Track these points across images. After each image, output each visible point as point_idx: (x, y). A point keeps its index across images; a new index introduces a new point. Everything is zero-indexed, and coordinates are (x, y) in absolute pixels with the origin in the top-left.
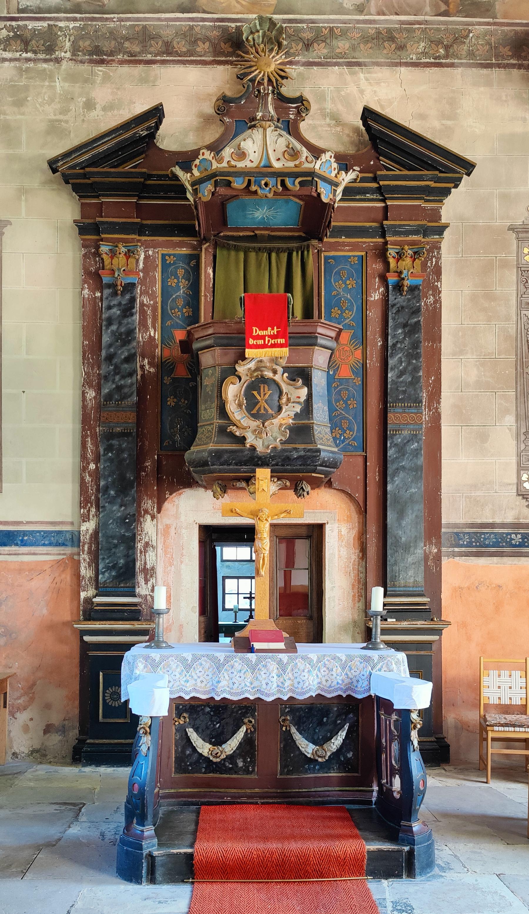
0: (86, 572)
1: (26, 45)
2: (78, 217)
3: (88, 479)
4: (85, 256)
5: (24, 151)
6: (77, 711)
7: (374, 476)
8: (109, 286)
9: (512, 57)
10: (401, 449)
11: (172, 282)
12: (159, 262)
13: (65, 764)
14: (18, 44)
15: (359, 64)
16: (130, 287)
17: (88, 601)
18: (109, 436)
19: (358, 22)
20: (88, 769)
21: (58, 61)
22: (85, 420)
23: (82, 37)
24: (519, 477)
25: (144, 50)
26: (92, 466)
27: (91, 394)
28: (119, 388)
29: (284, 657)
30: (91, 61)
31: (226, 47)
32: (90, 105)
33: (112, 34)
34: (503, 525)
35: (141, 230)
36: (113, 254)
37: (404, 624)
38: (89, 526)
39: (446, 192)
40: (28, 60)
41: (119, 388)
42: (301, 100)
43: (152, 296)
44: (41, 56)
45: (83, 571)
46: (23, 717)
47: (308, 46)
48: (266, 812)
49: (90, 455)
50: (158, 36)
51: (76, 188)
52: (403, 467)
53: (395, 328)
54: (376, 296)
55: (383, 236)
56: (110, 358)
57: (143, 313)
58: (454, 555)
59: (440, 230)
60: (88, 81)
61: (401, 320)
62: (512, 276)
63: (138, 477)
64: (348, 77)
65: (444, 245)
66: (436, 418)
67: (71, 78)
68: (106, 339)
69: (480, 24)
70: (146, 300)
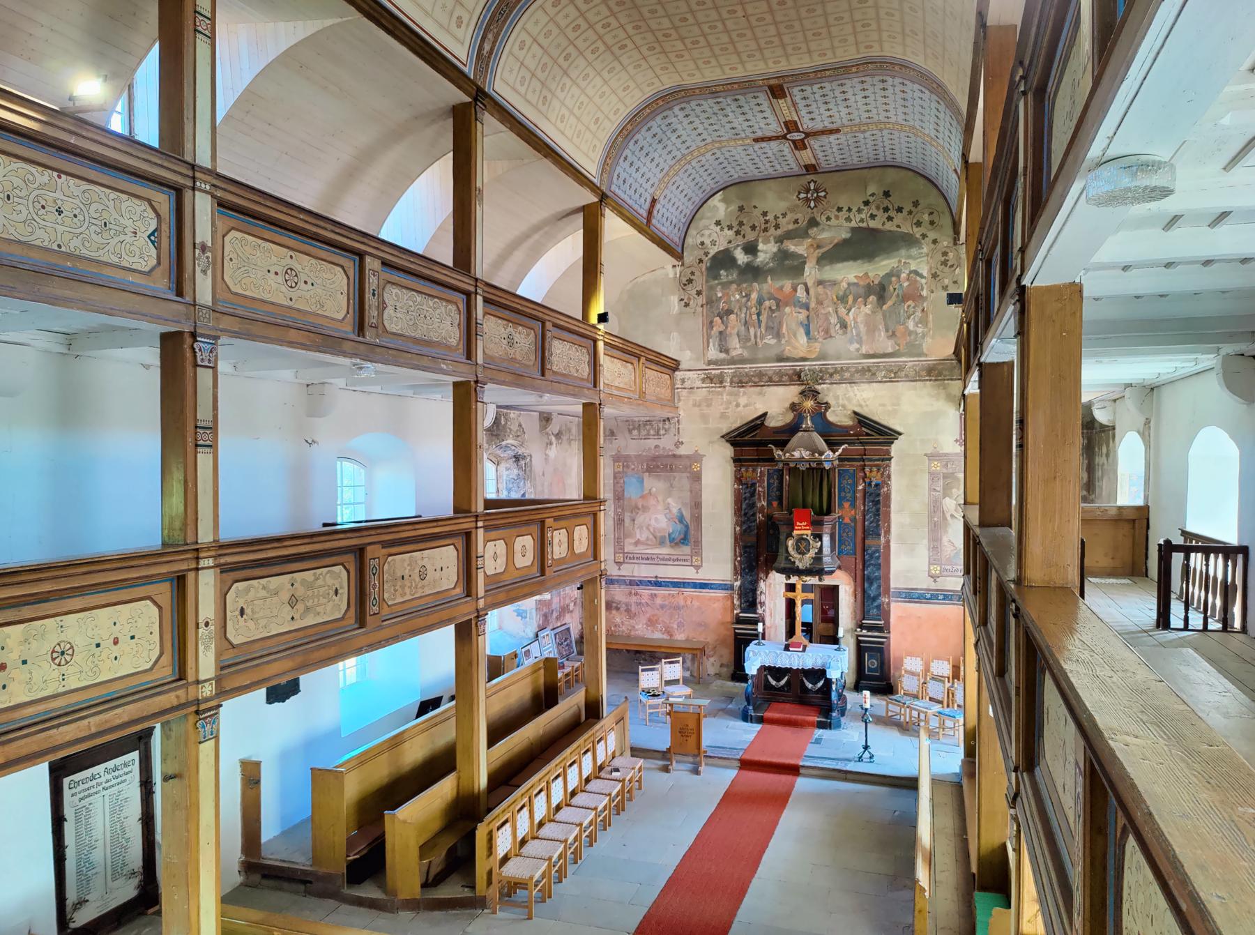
0: (736, 602)
1: (712, 381)
2: (733, 456)
3: (737, 564)
4: (735, 471)
5: (710, 426)
7: (860, 566)
8: (745, 484)
9: (927, 376)
10: (871, 556)
11: (772, 481)
12: (766, 473)
14: (708, 381)
15: (854, 383)
16: (753, 485)
17: (737, 614)
18: (745, 547)
20: (737, 684)
21: (724, 387)
22: (736, 539)
24: (929, 567)
25: (761, 381)
26: (739, 559)
27: (738, 528)
28: (749, 527)
30: (738, 387)
31: (796, 378)
32: (738, 405)
33: (747, 375)
34: (921, 589)
35: (758, 460)
36: (747, 471)
37: (870, 634)
38: (737, 584)
39: (892, 443)
41: (749, 527)
42: (827, 403)
44: (718, 385)
45: (735, 602)
46: (712, 660)
47: (831, 375)
49: (738, 554)
50: (766, 374)
51: (732, 444)
52: (872, 564)
53: (869, 503)
55: (864, 461)
56: (745, 514)
57: (759, 494)
59: (890, 459)
60: (737, 395)
61: (872, 499)
62: (926, 476)
63: (757, 563)
64: (850, 389)
66: (888, 542)
67: (730, 394)
68: (744, 506)
69: (911, 361)
70: (760, 489)
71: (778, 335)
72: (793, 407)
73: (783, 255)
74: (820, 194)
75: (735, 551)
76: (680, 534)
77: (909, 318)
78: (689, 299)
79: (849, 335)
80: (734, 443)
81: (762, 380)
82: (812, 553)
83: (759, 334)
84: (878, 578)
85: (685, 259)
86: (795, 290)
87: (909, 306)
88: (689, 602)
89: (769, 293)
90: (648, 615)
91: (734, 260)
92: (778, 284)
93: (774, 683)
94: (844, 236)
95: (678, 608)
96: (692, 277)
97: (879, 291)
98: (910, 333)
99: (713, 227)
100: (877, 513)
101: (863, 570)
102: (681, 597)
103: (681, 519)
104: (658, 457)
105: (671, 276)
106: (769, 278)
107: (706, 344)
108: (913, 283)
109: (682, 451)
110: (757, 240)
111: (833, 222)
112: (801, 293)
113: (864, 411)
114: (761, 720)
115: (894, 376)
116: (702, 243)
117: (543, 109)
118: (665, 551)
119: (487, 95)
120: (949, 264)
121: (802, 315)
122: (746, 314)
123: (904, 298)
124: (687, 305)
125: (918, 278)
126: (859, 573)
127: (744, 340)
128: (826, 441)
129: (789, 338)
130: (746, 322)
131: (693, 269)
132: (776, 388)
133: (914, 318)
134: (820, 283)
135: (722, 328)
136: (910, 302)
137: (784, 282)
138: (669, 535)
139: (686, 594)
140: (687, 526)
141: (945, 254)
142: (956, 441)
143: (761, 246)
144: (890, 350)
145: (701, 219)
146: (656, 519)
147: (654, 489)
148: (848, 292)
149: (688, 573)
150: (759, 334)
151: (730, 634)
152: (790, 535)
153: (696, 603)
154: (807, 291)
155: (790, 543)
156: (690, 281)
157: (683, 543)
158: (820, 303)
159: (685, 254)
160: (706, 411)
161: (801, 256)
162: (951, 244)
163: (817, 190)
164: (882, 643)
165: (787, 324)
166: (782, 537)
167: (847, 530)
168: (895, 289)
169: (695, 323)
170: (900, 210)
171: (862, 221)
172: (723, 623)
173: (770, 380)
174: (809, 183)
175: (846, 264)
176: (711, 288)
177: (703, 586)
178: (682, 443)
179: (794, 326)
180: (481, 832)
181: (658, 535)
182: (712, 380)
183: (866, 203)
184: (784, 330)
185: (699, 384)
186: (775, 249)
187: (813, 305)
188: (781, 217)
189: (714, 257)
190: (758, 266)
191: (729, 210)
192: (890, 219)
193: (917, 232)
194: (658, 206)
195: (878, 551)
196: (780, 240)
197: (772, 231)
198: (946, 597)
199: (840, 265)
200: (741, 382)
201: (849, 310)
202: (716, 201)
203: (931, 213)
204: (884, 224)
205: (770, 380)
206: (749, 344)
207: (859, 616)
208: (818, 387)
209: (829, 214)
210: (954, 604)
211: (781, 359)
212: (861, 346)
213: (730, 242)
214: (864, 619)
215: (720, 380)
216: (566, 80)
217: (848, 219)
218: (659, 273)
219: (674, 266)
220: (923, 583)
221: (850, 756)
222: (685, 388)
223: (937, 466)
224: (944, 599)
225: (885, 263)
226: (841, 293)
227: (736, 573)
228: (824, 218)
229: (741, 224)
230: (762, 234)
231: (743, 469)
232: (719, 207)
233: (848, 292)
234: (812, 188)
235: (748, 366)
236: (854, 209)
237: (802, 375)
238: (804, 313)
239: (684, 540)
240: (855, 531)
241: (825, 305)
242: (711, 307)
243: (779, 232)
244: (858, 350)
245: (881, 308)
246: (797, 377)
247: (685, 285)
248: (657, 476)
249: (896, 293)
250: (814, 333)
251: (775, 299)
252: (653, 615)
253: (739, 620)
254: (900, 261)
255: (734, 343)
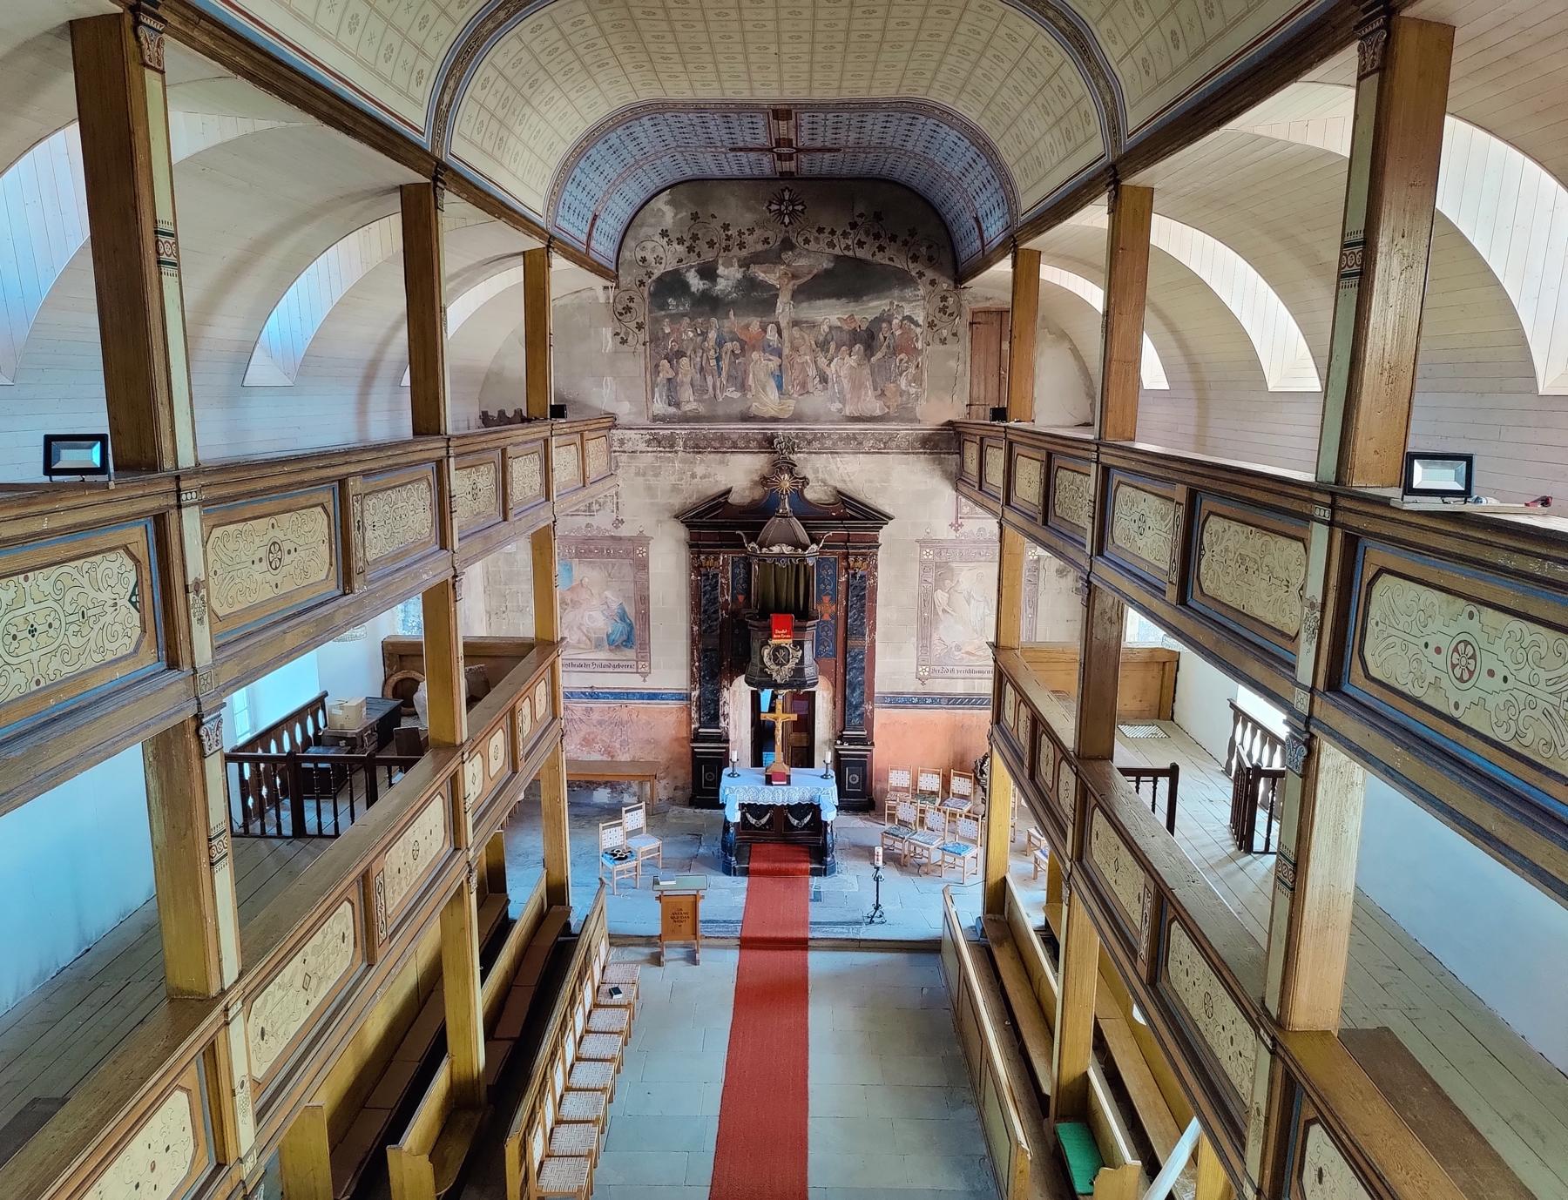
0: (695, 715)
6: (690, 780)
10: (854, 658)
11: (737, 571)
13: (684, 805)
15: (837, 453)
16: (715, 576)
18: (705, 650)
19: (837, 429)
21: (676, 452)
22: (693, 641)
23: (689, 439)
26: (697, 664)
27: (696, 628)
28: (710, 626)
29: (784, 788)
32: (693, 476)
34: (908, 693)
36: (707, 559)
37: (852, 747)
38: (695, 693)
40: (661, 452)
41: (710, 626)
42: (804, 478)
43: (727, 579)
46: (663, 782)
47: (809, 443)
48: (777, 847)
50: (729, 438)
51: (687, 526)
53: (853, 597)
54: (843, 579)
55: (847, 549)
56: (705, 611)
58: (883, 707)
59: (877, 547)
62: (917, 566)
65: (880, 552)
66: (873, 642)
67: (683, 461)
68: (703, 602)
71: (743, 387)
72: (764, 481)
73: (749, 284)
74: (796, 208)
75: (692, 653)
76: (622, 634)
77: (901, 375)
78: (627, 334)
79: (830, 392)
80: (689, 525)
81: (725, 446)
82: (792, 664)
83: (718, 384)
84: (861, 684)
85: (621, 279)
86: (765, 331)
87: (901, 360)
88: (634, 716)
89: (731, 332)
90: (582, 734)
91: (685, 286)
92: (745, 321)
93: (753, 821)
94: (825, 266)
95: (620, 724)
96: (631, 305)
97: (867, 339)
98: (902, 393)
99: (657, 238)
100: (862, 610)
101: (845, 675)
102: (625, 710)
103: (623, 617)
104: (590, 538)
105: (602, 300)
106: (732, 312)
107: (650, 396)
108: (906, 332)
109: (624, 531)
110: (715, 261)
111: (813, 246)
112: (771, 334)
113: (848, 488)
114: (746, 872)
115: (883, 446)
116: (644, 260)
117: (497, 154)
118: (602, 655)
119: (446, 167)
120: (949, 311)
121: (774, 363)
122: (702, 357)
123: (894, 351)
124: (624, 341)
125: (913, 326)
126: (839, 677)
127: (700, 390)
128: (803, 525)
129: (758, 392)
130: (702, 368)
131: (632, 294)
132: (741, 456)
133: (907, 375)
134: (796, 323)
135: (671, 374)
136: (902, 356)
137: (750, 319)
138: (608, 636)
139: (630, 707)
140: (630, 625)
141: (944, 299)
142: (951, 525)
143: (721, 270)
144: (878, 413)
145: (641, 226)
146: (590, 617)
147: (587, 580)
148: (829, 337)
149: (632, 682)
150: (718, 384)
151: (686, 750)
152: (765, 644)
153: (643, 717)
154: (780, 333)
155: (766, 652)
156: (628, 309)
157: (626, 646)
158: (795, 349)
159: (620, 272)
160: (653, 481)
161: (773, 286)
162: (951, 288)
163: (792, 202)
164: (865, 756)
165: (754, 374)
166: (755, 645)
167: (826, 629)
168: (885, 338)
169: (635, 365)
170: (893, 239)
171: (847, 248)
172: (677, 739)
173: (735, 445)
174: (783, 191)
175: (827, 301)
176: (656, 321)
177: (653, 696)
178: (622, 522)
179: (762, 375)
180: (512, 1148)
181: (593, 635)
182: (659, 443)
183: (853, 226)
184: (751, 381)
185: (642, 446)
186: (739, 276)
187: (786, 351)
188: (747, 233)
189: (660, 279)
190: (717, 295)
191: (679, 216)
192: (881, 249)
193: (914, 269)
194: (598, 222)
195: (862, 653)
196: (745, 264)
197: (735, 250)
198: (934, 701)
199: (819, 303)
200: (697, 446)
201: (831, 361)
202: (661, 203)
203: (929, 247)
204: (874, 255)
205: (735, 445)
206: (706, 397)
207: (839, 727)
208: (794, 457)
209: (808, 235)
210: (942, 708)
211: (746, 418)
212: (844, 406)
213: (680, 261)
214: (844, 730)
215: (670, 443)
216: (527, 110)
217: (831, 245)
218: (585, 295)
219: (606, 288)
220: (911, 686)
221: (858, 916)
222: (625, 452)
223: (928, 555)
224: (931, 703)
225: (872, 304)
226: (821, 338)
227: (693, 679)
228: (801, 239)
229: (695, 237)
230: (722, 254)
231: (702, 557)
232: (666, 213)
233: (829, 337)
234: (787, 198)
235: (706, 426)
236: (839, 232)
237: (775, 442)
238: (776, 361)
239: (628, 642)
240: (836, 629)
241: (802, 353)
242: (657, 346)
243: (744, 253)
244: (840, 411)
245: (869, 361)
246: (768, 443)
247: (621, 314)
248: (590, 562)
249: (886, 343)
250: (787, 386)
251: (739, 340)
252: (589, 734)
253: (697, 738)
254: (892, 303)
255: (687, 394)
